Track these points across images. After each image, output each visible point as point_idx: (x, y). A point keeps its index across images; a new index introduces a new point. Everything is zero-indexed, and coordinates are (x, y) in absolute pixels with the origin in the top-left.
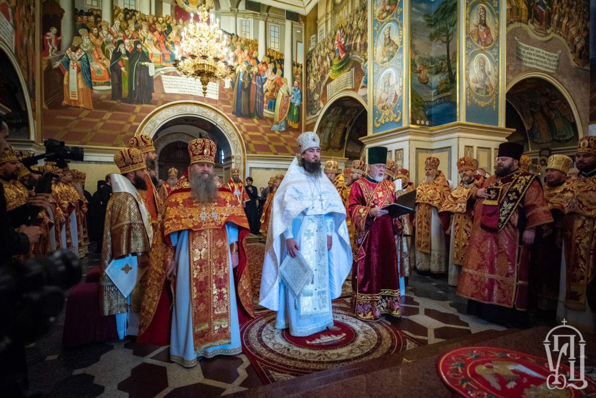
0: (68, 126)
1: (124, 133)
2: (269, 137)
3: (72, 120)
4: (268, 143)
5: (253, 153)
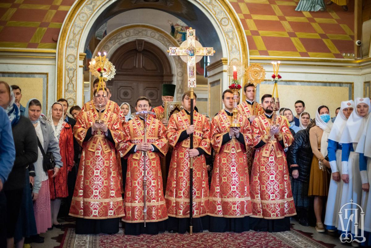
2: (290, 23)
4: (288, 33)
5: (262, 53)
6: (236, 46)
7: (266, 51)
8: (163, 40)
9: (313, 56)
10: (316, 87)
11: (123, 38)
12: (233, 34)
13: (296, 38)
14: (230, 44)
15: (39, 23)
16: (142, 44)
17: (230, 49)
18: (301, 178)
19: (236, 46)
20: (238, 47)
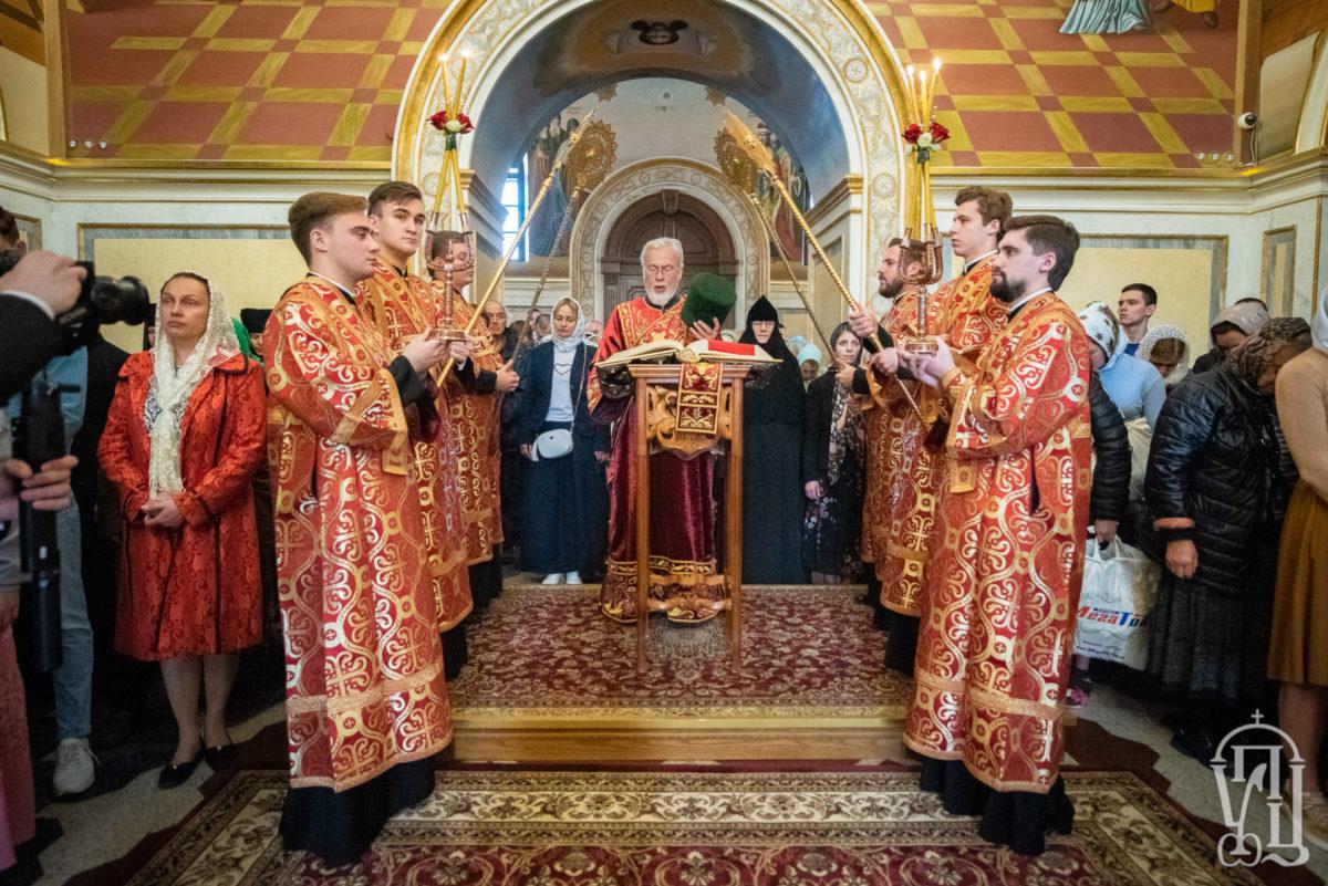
0: (158, 81)
1: (369, 95)
4: (1039, 99)
6: (887, 139)
7: (973, 154)
8: (717, 190)
9: (1105, 160)
10: (1115, 250)
11: (635, 188)
12: (878, 103)
13: (1059, 113)
14: (870, 134)
15: (350, 91)
16: (673, 199)
17: (871, 148)
18: (1206, 575)
19: (887, 139)
20: (892, 143)
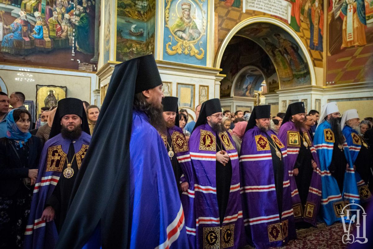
0: (345, 67)
3: (347, 61)
